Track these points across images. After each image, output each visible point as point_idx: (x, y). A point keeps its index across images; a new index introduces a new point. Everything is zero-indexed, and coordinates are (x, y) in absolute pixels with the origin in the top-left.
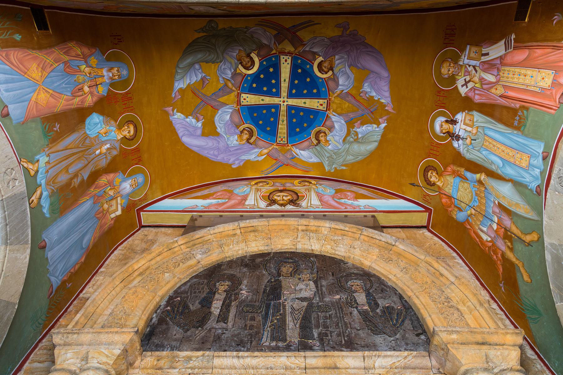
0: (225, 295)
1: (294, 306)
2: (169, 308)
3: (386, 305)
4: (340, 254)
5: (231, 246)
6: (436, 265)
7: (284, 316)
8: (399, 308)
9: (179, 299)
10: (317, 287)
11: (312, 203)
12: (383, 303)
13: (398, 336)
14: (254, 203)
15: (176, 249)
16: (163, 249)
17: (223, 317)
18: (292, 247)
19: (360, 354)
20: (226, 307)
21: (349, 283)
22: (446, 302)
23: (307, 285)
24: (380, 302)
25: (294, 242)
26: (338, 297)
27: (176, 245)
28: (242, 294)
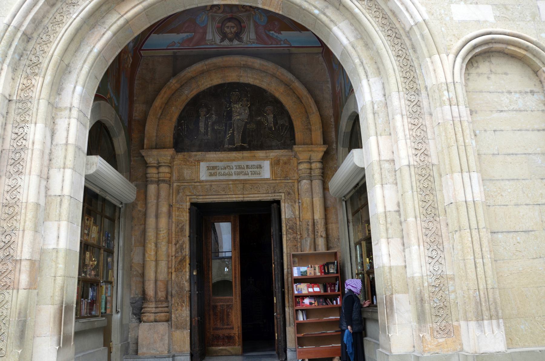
0: (205, 118)
1: (239, 124)
2: (180, 128)
3: (281, 123)
4: (263, 86)
5: (203, 82)
6: (310, 100)
7: (233, 130)
8: (287, 125)
9: (183, 121)
10: (250, 111)
11: (251, 37)
12: (280, 122)
13: (282, 142)
14: (211, 38)
15: (173, 87)
16: (166, 89)
17: (206, 133)
18: (238, 80)
19: (265, 151)
20: (206, 125)
21: (266, 108)
22: (306, 126)
23: (245, 110)
24: (279, 122)
25: (239, 76)
26: (259, 118)
27: (172, 84)
28: (213, 117)
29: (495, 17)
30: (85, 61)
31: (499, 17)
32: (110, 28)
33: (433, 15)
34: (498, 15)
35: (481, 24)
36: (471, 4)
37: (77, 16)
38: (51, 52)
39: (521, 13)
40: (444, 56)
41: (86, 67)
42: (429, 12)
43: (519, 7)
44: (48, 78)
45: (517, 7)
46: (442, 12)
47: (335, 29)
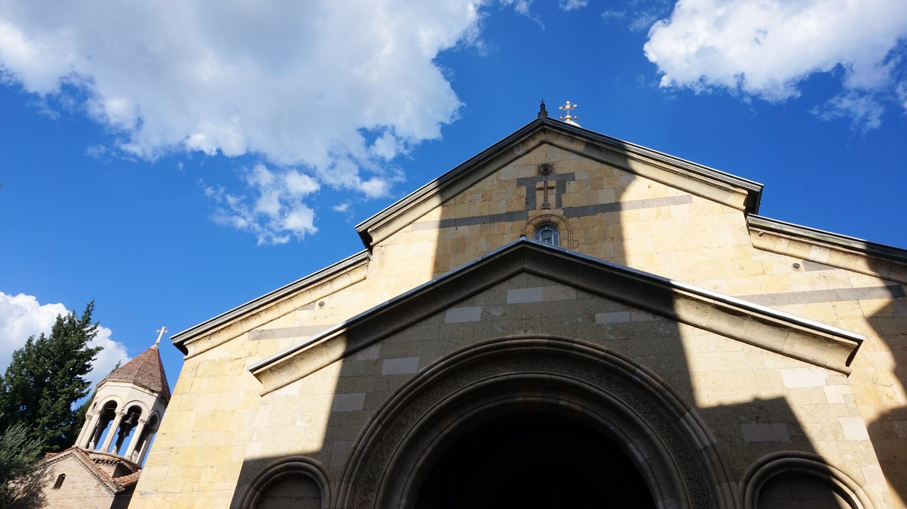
29: (791, 437)
30: (409, 476)
31: (795, 436)
32: (431, 443)
33: (722, 437)
34: (794, 434)
35: (776, 446)
36: (763, 423)
37: (406, 436)
38: (384, 470)
39: (821, 432)
40: (733, 483)
41: (410, 480)
42: (719, 435)
43: (818, 425)
44: (381, 494)
45: (816, 425)
46: (732, 433)
47: (631, 446)
